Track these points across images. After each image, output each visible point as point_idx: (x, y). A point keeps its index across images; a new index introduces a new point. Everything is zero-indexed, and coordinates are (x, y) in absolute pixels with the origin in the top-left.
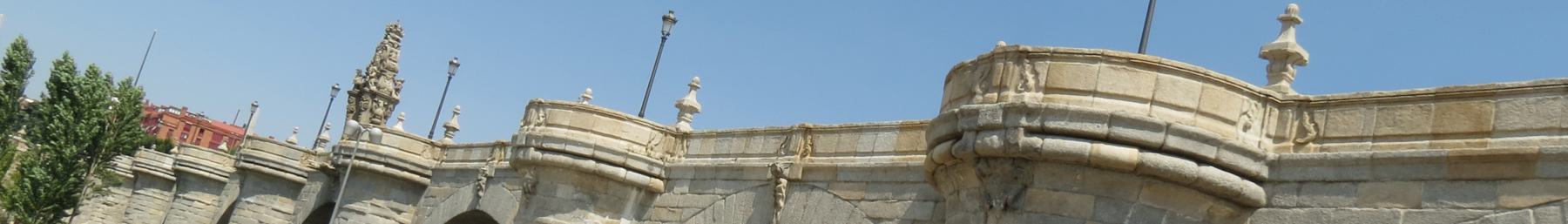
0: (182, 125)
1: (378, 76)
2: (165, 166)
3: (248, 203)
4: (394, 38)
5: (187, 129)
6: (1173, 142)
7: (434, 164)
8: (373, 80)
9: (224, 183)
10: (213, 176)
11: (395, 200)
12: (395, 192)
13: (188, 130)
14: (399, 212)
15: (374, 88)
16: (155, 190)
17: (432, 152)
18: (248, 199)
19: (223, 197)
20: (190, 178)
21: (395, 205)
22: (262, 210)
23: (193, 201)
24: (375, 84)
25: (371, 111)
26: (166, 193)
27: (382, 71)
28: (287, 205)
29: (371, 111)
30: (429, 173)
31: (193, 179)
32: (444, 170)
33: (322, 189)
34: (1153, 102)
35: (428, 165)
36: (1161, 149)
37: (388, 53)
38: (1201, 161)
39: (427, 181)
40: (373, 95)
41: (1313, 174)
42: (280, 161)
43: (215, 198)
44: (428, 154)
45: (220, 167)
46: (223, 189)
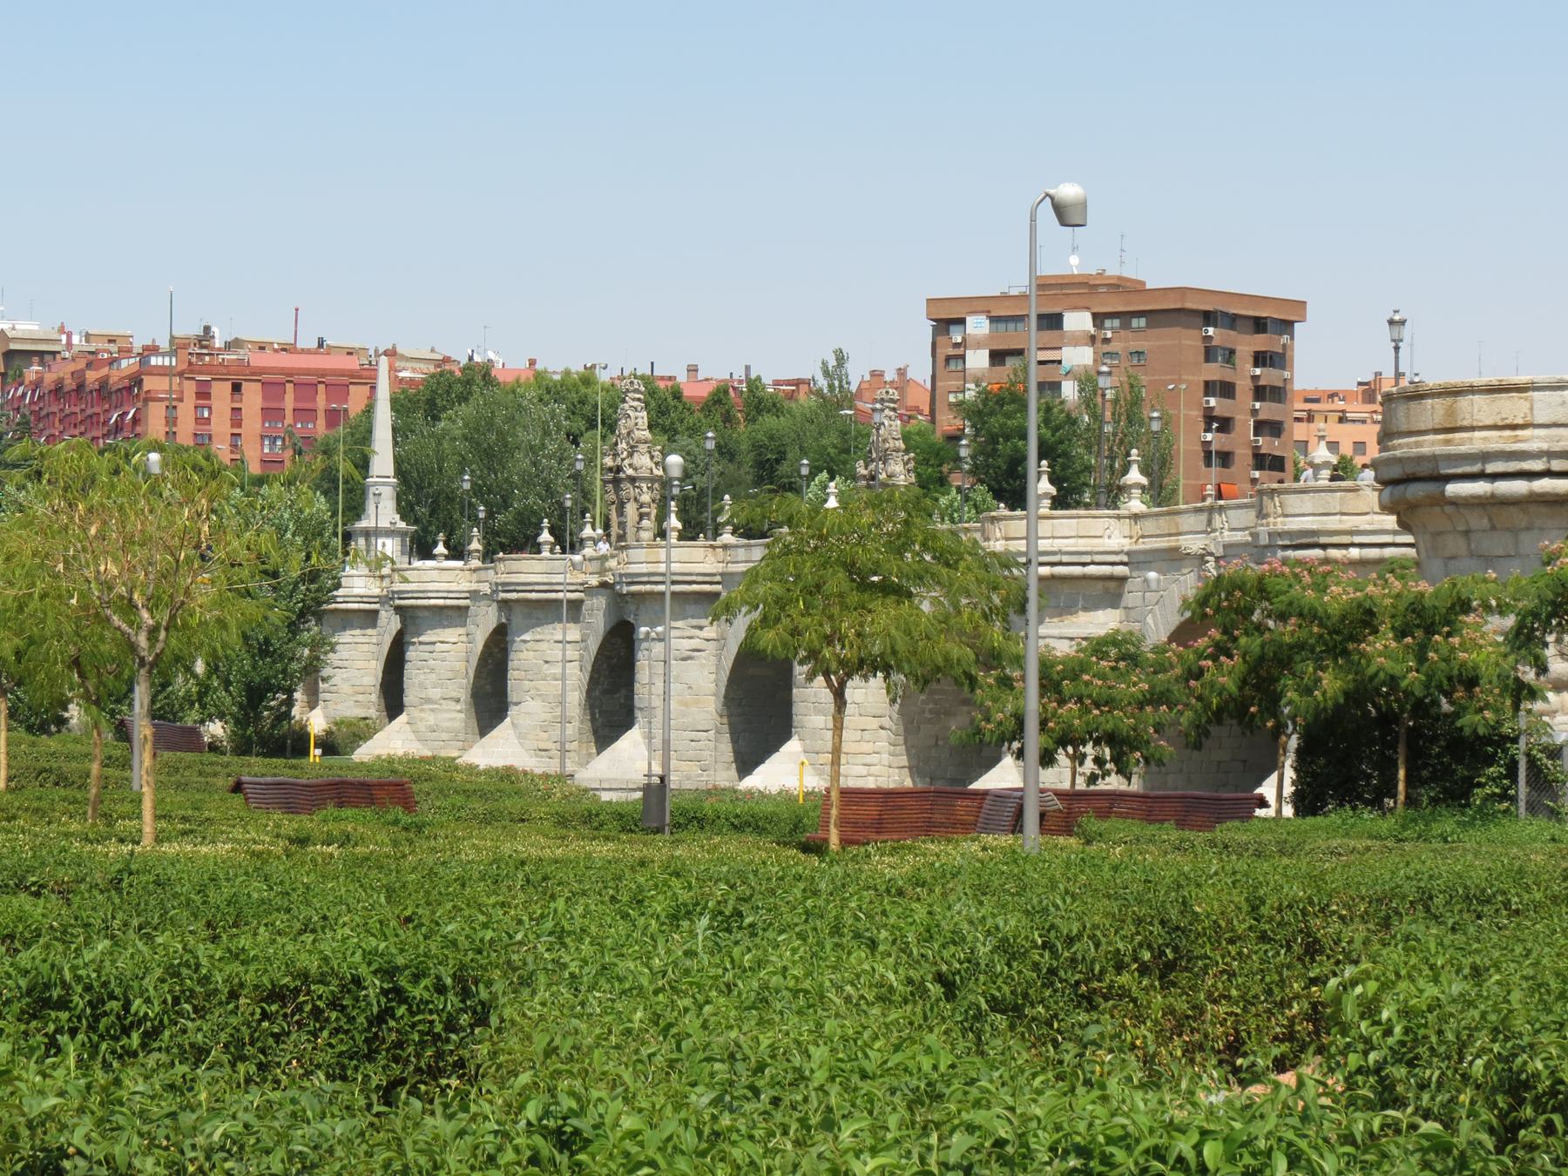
0: (190, 388)
1: (631, 455)
2: (356, 591)
3: (525, 642)
4: (634, 399)
5: (203, 394)
6: (1065, 559)
7: (720, 568)
8: (626, 462)
9: (467, 608)
10: (449, 602)
11: (693, 617)
12: (690, 608)
13: (207, 396)
14: (701, 628)
15: (630, 472)
16: (353, 632)
17: (715, 555)
18: (523, 637)
19: (472, 628)
20: (420, 614)
21: (695, 622)
22: (543, 646)
23: (434, 643)
24: (630, 465)
25: (636, 499)
26: (370, 631)
27: (632, 447)
28: (574, 632)
29: (636, 499)
30: (718, 578)
31: (426, 614)
32: (732, 574)
33: (608, 604)
34: (1054, 537)
35: (714, 571)
36: (1061, 564)
37: (633, 421)
38: (1084, 564)
39: (718, 588)
40: (632, 480)
41: (1142, 558)
42: (545, 580)
43: (461, 631)
44: (711, 559)
45: (454, 587)
46: (467, 616)
